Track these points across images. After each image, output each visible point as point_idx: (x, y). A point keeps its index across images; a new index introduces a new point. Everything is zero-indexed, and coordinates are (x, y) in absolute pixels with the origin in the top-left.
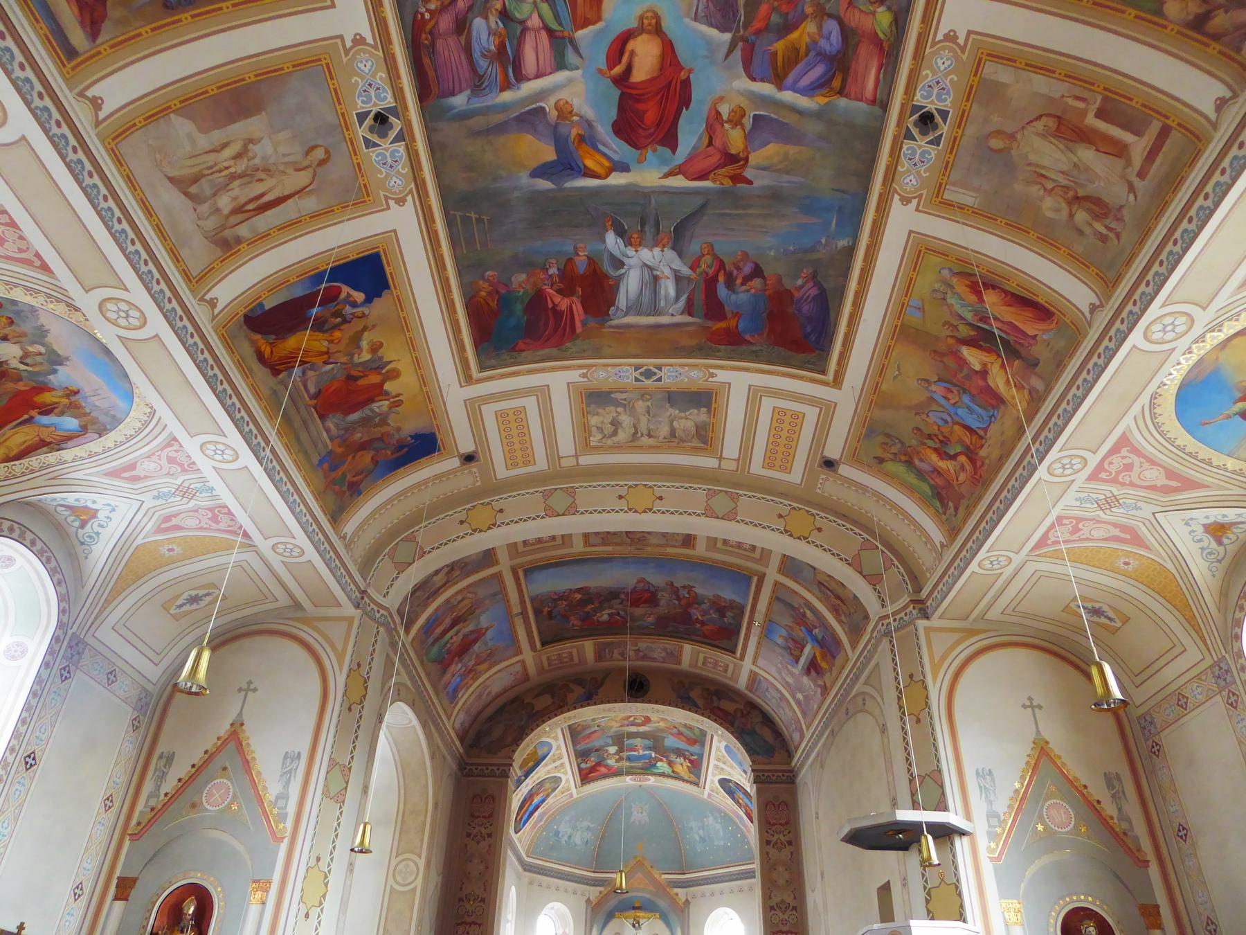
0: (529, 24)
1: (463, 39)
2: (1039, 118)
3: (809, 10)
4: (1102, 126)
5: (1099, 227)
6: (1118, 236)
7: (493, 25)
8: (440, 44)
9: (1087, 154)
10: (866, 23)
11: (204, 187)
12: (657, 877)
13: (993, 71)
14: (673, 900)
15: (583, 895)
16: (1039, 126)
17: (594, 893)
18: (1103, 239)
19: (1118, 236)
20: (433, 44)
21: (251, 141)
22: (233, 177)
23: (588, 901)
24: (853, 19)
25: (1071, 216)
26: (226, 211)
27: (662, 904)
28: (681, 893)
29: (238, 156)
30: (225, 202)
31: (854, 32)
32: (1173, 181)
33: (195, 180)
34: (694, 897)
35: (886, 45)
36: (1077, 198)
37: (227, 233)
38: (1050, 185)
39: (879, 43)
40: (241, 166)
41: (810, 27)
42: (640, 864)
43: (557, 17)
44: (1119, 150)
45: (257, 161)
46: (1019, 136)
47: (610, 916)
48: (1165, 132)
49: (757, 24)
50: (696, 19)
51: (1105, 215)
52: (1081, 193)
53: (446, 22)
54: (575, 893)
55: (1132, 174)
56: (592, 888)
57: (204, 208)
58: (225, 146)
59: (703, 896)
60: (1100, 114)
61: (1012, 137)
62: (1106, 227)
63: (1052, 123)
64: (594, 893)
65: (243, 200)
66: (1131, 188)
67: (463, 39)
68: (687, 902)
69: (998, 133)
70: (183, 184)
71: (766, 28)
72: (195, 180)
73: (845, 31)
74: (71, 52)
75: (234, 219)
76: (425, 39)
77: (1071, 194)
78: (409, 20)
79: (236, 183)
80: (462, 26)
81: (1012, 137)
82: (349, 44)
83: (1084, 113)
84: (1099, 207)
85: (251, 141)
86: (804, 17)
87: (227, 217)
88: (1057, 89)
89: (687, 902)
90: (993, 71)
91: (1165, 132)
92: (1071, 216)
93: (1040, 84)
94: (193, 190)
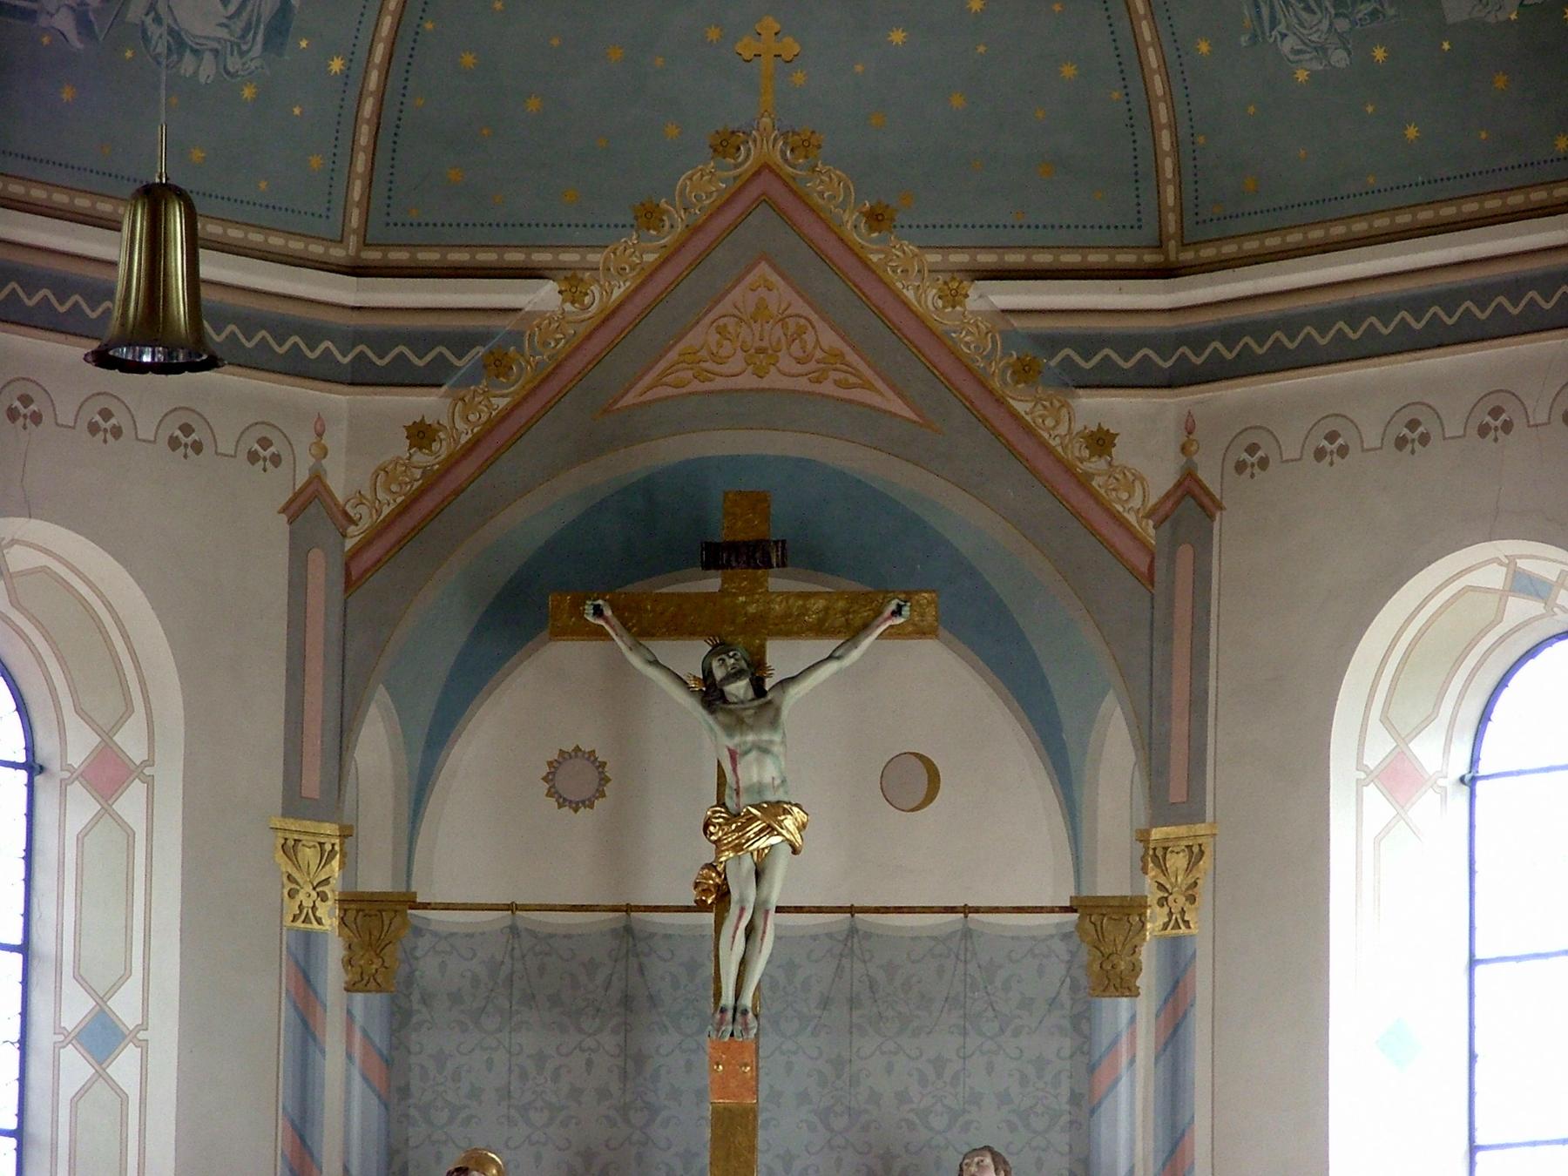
12: (926, 298)
14: (1066, 490)
15: (263, 454)
17: (357, 438)
23: (308, 503)
27: (968, 519)
28: (1143, 432)
34: (1252, 459)
42: (772, 199)
47: (521, 611)
54: (186, 439)
56: (338, 400)
59: (1332, 446)
64: (357, 438)
68: (1191, 504)
89: (1191, 504)
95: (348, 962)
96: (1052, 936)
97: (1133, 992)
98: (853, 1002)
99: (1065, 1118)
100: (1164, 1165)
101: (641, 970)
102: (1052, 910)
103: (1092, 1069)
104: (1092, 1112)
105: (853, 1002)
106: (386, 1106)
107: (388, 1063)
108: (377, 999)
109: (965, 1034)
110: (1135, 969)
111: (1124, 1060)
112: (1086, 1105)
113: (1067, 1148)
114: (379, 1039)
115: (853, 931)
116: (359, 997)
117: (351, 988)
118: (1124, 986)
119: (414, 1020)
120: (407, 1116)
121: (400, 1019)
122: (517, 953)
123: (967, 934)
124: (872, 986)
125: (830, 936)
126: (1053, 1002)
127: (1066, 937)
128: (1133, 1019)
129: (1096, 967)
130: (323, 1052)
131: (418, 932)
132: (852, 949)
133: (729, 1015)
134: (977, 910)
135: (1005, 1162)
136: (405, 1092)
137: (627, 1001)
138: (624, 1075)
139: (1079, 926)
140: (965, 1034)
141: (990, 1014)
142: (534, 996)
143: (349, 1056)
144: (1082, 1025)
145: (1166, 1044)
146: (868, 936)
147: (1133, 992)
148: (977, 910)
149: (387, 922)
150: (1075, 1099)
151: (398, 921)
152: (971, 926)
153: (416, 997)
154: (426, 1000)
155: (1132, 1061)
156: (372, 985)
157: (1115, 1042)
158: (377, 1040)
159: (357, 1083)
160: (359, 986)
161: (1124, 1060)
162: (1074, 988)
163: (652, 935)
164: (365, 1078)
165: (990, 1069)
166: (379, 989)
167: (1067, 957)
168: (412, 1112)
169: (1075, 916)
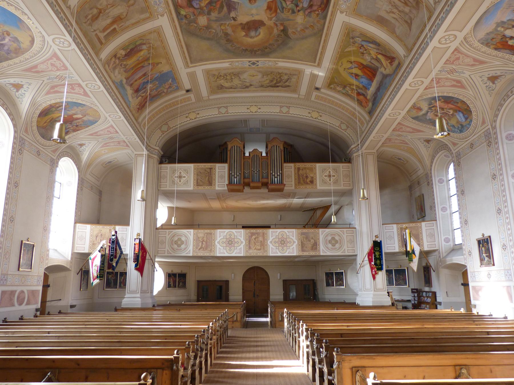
0: (290, 3)
1: (312, 3)
2: (126, 15)
3: (205, 8)
4: (112, 28)
5: (90, 17)
6: (85, 23)
7: (301, 4)
8: (319, 4)
9: (109, 21)
10: (187, 10)
11: (407, 18)
13: (148, 15)
16: (125, 14)
18: (86, 17)
19: (85, 23)
20: (321, 4)
21: (387, 12)
22: (399, 11)
24: (191, 10)
25: (97, 8)
26: (409, 8)
29: (393, 13)
30: (407, 9)
31: (189, 7)
32: (90, 42)
33: (406, 22)
35: (179, 7)
36: (100, 12)
37: (414, 4)
38: (109, 6)
39: (181, 7)
40: (395, 10)
41: (203, 5)
43: (281, 3)
44: (104, 30)
45: (390, 7)
46: (127, 8)
48: (101, 43)
49: (219, 3)
50: (238, 3)
51: (92, 20)
52: (101, 14)
53: (315, 8)
55: (97, 32)
57: (412, 16)
58: (394, 18)
60: (115, 29)
61: (129, 7)
62: (88, 20)
63: (122, 17)
65: (403, 4)
66: (95, 31)
67: (312, 3)
69: (133, 5)
70: (410, 25)
71: (216, 2)
72: (406, 22)
73: (192, 6)
74: (399, 64)
75: (409, 4)
76: (323, 6)
77: (103, 11)
78: (325, 12)
79: (400, 9)
80: (311, 6)
81: (129, 7)
82: (345, 13)
83: (118, 25)
84: (95, 18)
85: (387, 12)
86: (205, 6)
87: (410, 7)
88: (128, 23)
90: (148, 15)
91: (101, 43)
92: (97, 8)
93: (133, 21)
94: (409, 22)
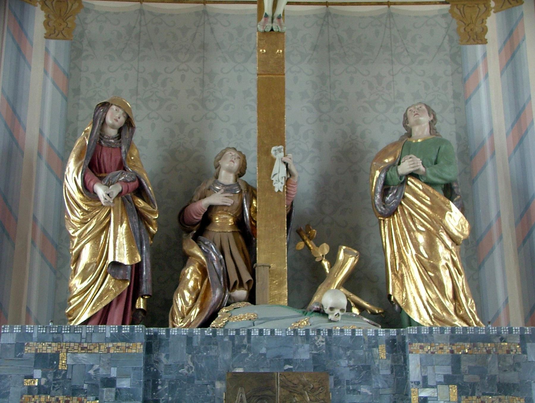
95: (46, 24)
96: (436, 16)
97: (484, 42)
98: (330, 47)
99: (452, 106)
100: (512, 126)
101: (212, 31)
102: (435, 3)
103: (464, 80)
104: (466, 102)
105: (330, 47)
106: (66, 99)
107: (68, 76)
108: (63, 44)
109: (392, 63)
110: (485, 30)
111: (482, 76)
112: (462, 98)
113: (454, 122)
114: (63, 63)
115: (328, 14)
116: (52, 42)
117: (48, 37)
118: (479, 38)
119: (84, 54)
120: (78, 104)
121: (76, 54)
122: (143, 23)
123: (390, 15)
124: (340, 40)
125: (315, 15)
126: (440, 48)
127: (444, 16)
128: (485, 56)
129: (462, 30)
130: (30, 68)
131: (88, 11)
132: (328, 22)
133: (270, 20)
134: (395, 4)
135: (433, 111)
136: (77, 91)
137: (204, 46)
138: (203, 83)
139: (451, 11)
140: (392, 63)
141: (405, 53)
142: (152, 44)
143: (46, 72)
144: (456, 59)
145: (507, 65)
146: (336, 16)
147: (484, 42)
148: (395, 4)
149: (70, 5)
150: (456, 96)
151: (77, 4)
152: (392, 11)
153: (85, 42)
154: (91, 44)
155: (486, 76)
156: (60, 36)
157: (476, 66)
158: (62, 65)
159: (50, 86)
160: (52, 36)
161: (482, 76)
162: (451, 40)
163: (218, 14)
164: (54, 83)
165: (407, 80)
166: (65, 38)
167: (445, 26)
168: (81, 102)
169: (448, 6)
